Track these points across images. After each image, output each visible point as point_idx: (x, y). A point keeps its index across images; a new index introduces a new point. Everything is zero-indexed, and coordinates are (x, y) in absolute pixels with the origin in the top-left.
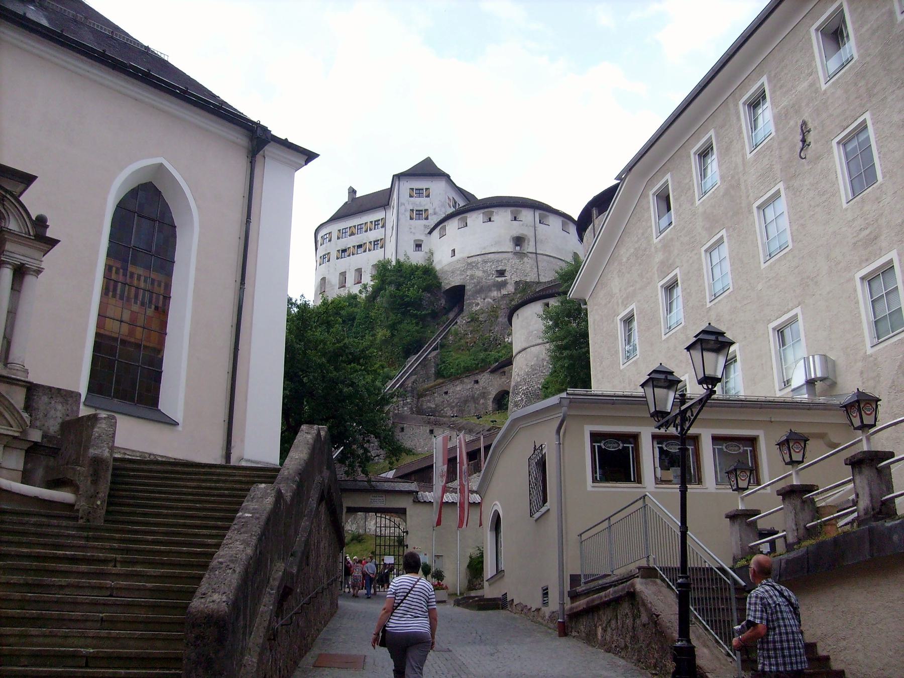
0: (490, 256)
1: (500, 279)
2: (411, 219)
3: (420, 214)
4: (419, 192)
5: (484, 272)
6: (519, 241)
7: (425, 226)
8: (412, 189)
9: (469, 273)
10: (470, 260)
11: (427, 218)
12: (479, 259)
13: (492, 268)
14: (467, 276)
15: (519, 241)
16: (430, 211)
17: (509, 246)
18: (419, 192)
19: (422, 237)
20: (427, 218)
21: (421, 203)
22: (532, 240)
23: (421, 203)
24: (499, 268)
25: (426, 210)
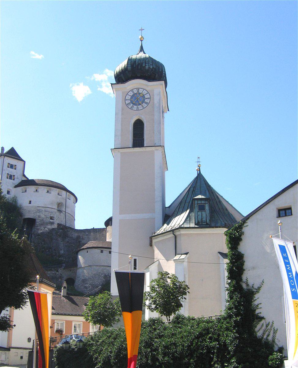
0: (48, 209)
1: (52, 221)
2: (7, 178)
3: (11, 177)
4: (12, 166)
5: (45, 215)
6: (59, 205)
7: (13, 183)
8: (9, 164)
9: (38, 214)
10: (39, 208)
11: (14, 180)
12: (43, 209)
13: (49, 215)
14: (37, 215)
15: (59, 205)
16: (16, 177)
17: (55, 207)
18: (12, 166)
19: (11, 188)
20: (14, 180)
21: (12, 171)
22: (65, 205)
23: (12, 171)
24: (51, 216)
25: (14, 176)
